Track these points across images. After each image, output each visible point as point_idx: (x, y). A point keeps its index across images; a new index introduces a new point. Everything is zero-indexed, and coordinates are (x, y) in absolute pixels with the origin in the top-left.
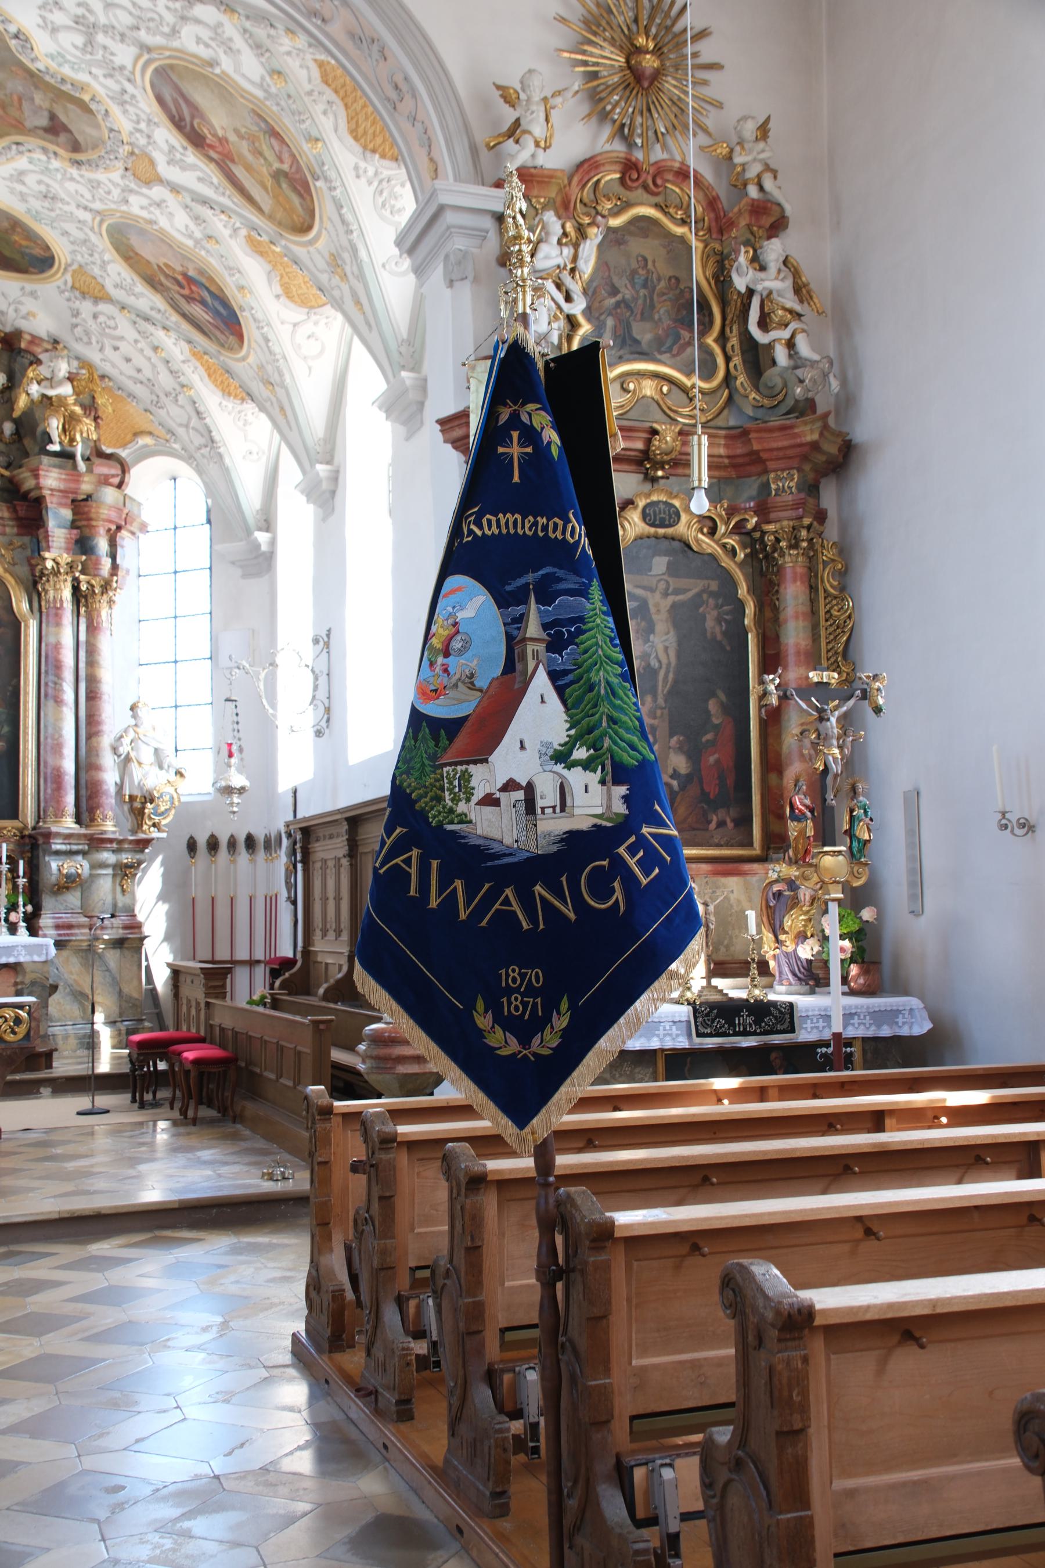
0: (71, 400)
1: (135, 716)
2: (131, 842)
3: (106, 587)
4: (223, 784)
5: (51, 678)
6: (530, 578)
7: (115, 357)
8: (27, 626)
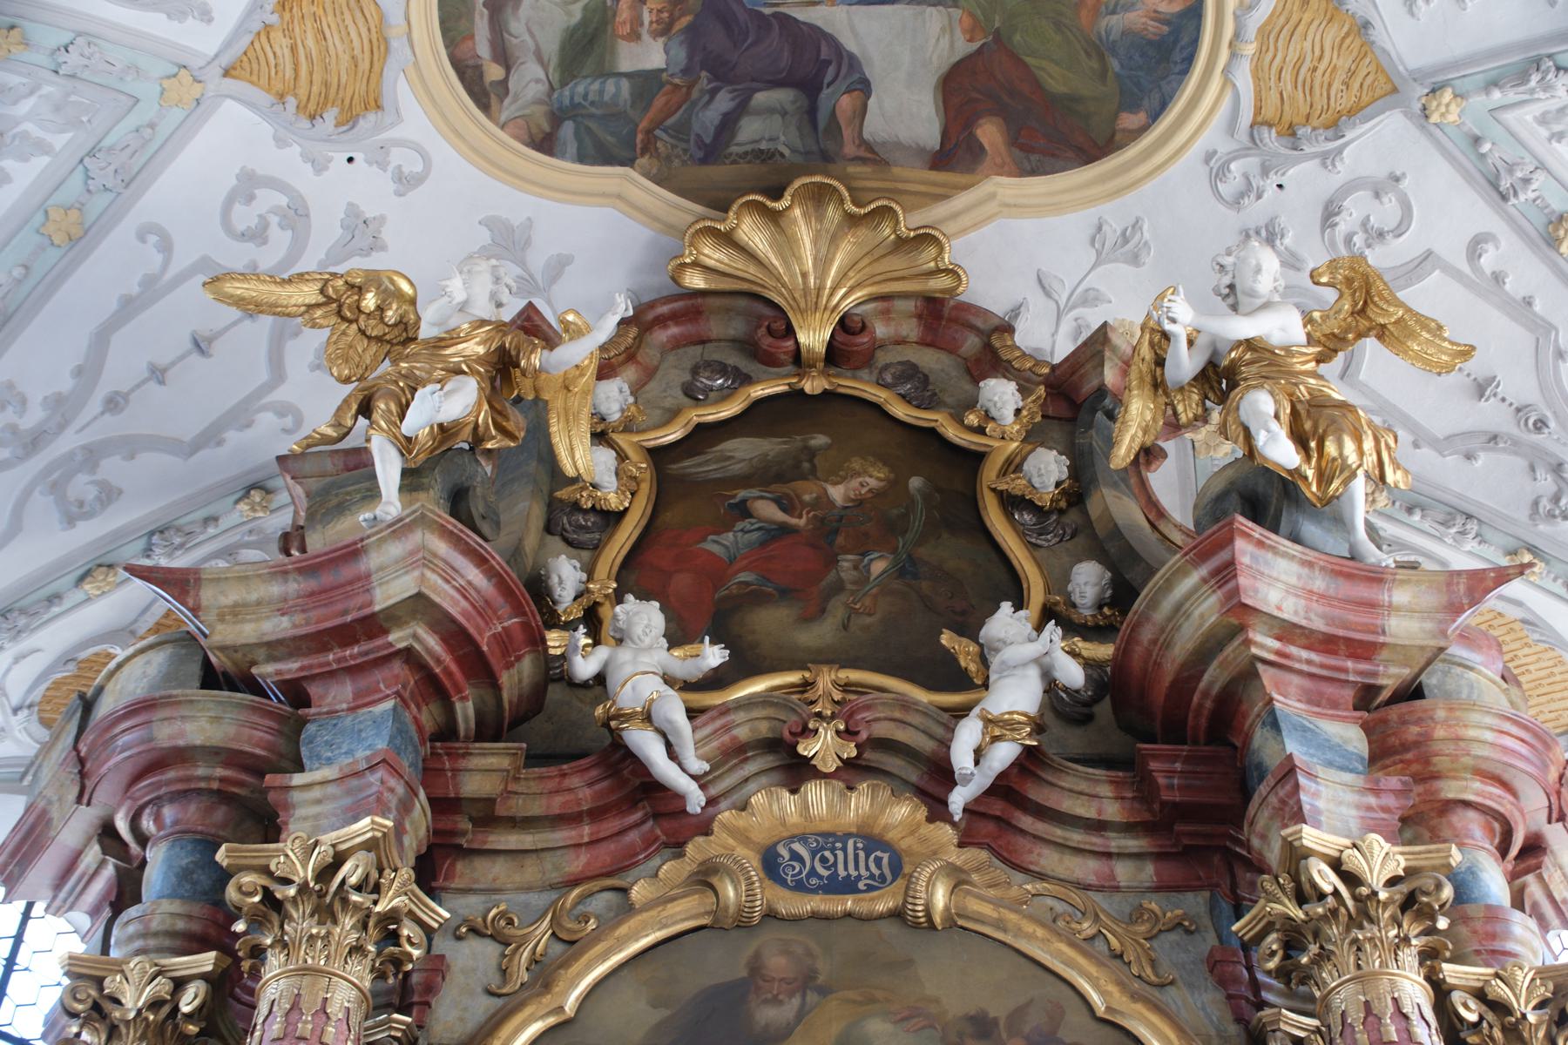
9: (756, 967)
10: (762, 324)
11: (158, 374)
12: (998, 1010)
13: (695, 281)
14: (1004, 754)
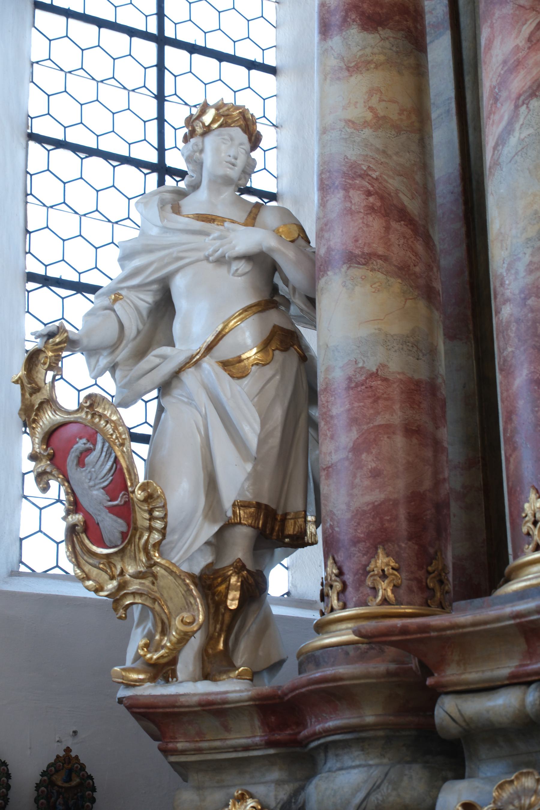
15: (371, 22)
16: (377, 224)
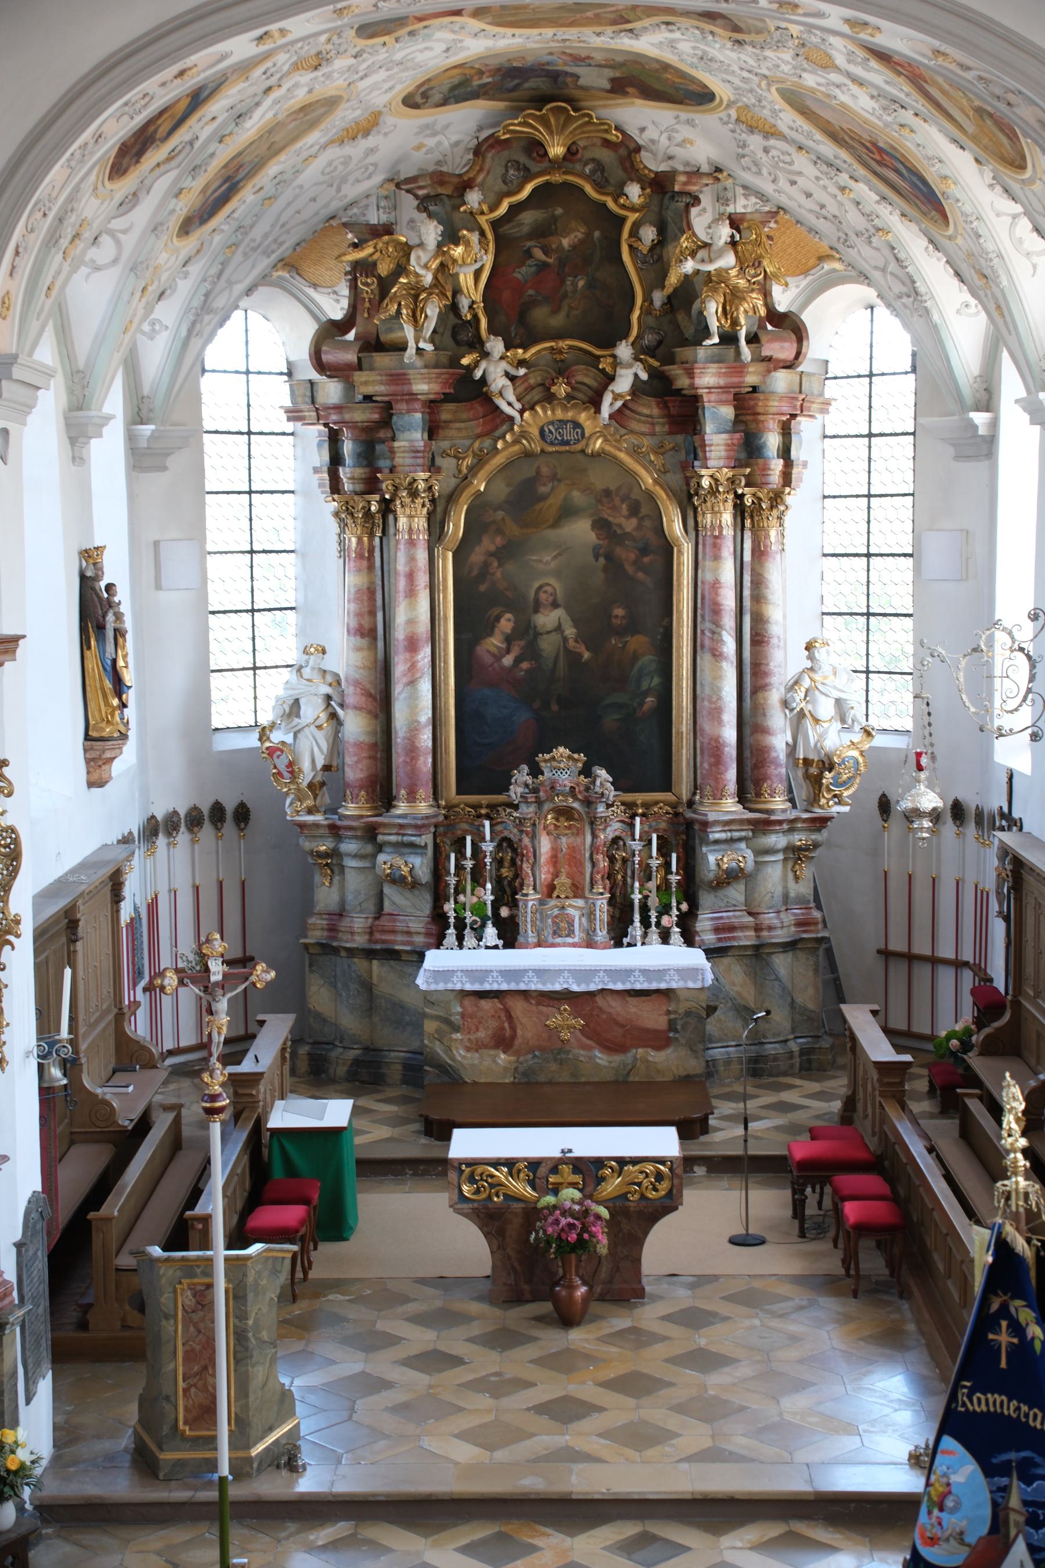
0: (733, 273)
1: (811, 658)
2: (805, 820)
3: (777, 499)
4: (910, 805)
5: (708, 625)
6: (1013, 1456)
7: (793, 191)
8: (680, 552)
9: (538, 472)
10: (535, 148)
11: (298, 212)
12: (612, 487)
13: (507, 136)
14: (619, 404)
15: (362, 635)
16: (364, 699)
